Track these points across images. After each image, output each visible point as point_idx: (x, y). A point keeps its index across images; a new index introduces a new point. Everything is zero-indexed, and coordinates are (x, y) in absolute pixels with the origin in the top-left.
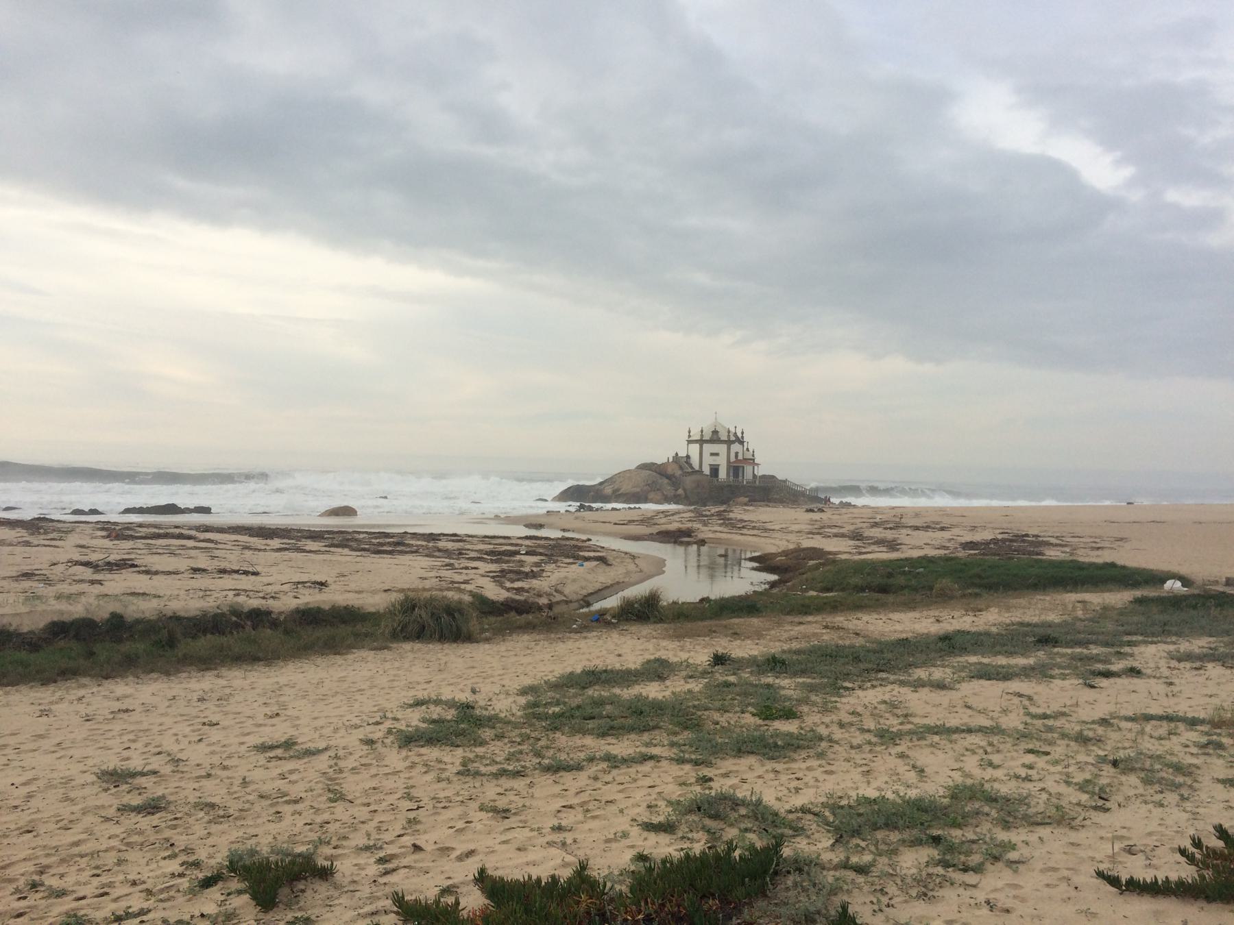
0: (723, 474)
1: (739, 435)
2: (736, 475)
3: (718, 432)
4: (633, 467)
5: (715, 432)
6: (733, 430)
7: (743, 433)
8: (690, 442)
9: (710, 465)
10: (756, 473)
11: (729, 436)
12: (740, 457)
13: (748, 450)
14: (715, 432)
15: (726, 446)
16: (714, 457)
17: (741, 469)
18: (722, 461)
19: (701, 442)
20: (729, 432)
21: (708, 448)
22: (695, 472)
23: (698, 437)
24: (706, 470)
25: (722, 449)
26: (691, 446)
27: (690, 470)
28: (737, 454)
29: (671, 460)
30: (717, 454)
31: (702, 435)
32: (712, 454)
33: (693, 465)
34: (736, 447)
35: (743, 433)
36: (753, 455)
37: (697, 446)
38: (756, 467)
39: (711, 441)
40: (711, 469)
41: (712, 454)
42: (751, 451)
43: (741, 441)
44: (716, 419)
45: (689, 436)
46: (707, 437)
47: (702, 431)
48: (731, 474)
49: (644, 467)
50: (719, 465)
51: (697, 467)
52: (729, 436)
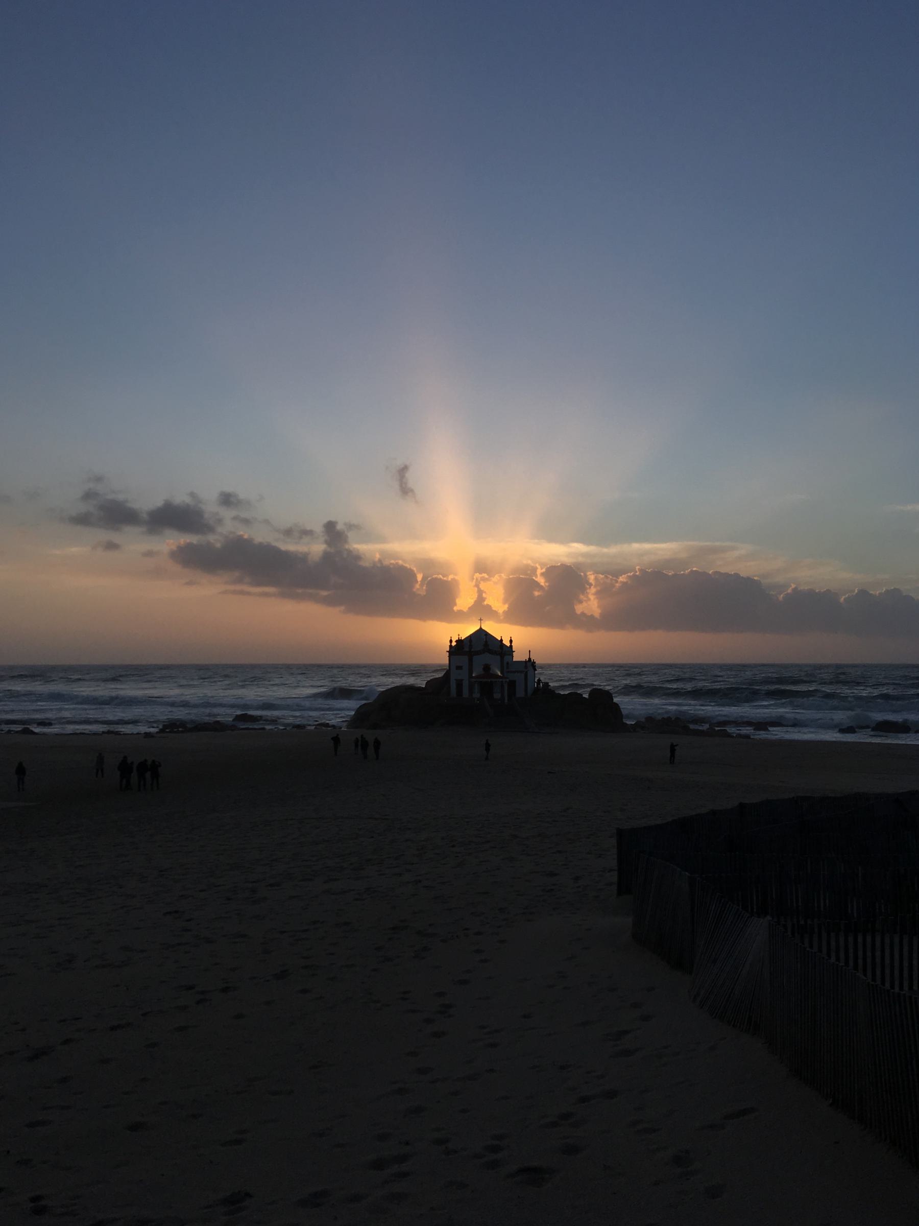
9: (456, 680)
11: (471, 647)
14: (459, 641)
25: (463, 660)
44: (481, 626)
50: (462, 680)
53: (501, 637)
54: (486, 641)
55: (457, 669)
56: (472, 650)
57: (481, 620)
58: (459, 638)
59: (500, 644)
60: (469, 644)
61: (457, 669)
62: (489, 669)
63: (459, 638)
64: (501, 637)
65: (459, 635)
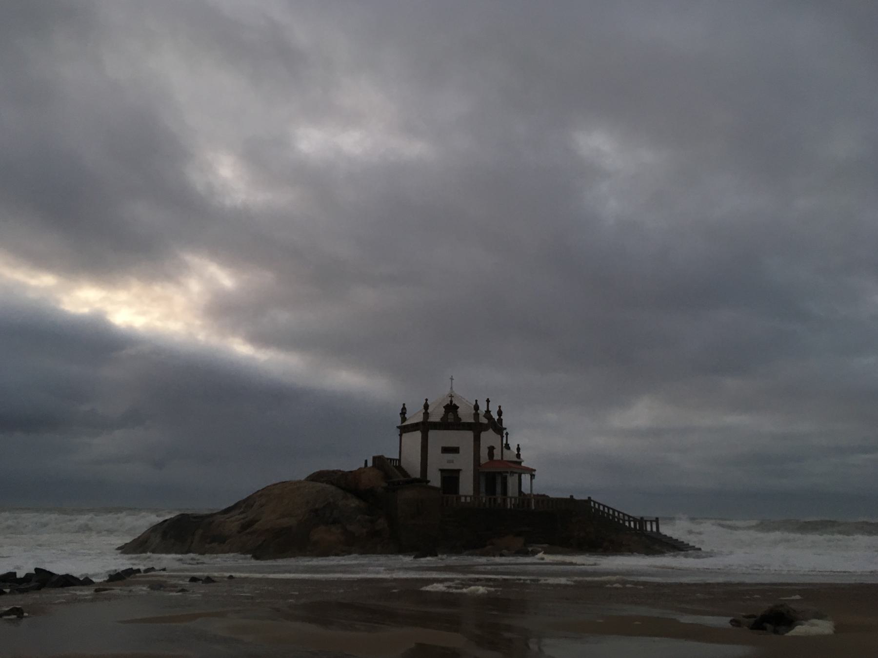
0: (466, 486)
1: (496, 417)
2: (491, 490)
3: (456, 407)
4: (303, 477)
5: (451, 408)
6: (483, 409)
7: (500, 413)
8: (404, 429)
9: (442, 471)
10: (526, 489)
11: (476, 415)
12: (497, 456)
13: (507, 447)
14: (451, 408)
15: (469, 435)
16: (450, 456)
17: (499, 481)
18: (464, 463)
19: (425, 427)
20: (476, 407)
21: (438, 439)
22: (412, 482)
23: (419, 419)
24: (435, 480)
25: (463, 439)
26: (406, 436)
27: (402, 478)
28: (491, 449)
29: (370, 464)
30: (455, 450)
31: (426, 414)
32: (446, 450)
33: (410, 472)
34: (489, 438)
35: (500, 413)
36: (518, 456)
37: (418, 435)
38: (526, 478)
39: (443, 425)
40: (444, 480)
41: (446, 450)
42: (514, 449)
43: (498, 427)
45: (404, 419)
46: (436, 415)
47: (426, 407)
48: (483, 489)
49: (319, 477)
50: (458, 471)
51: (415, 471)
52: (476, 415)
53: (500, 407)
54: (488, 412)
55: (442, 452)
56: (480, 422)
57: (452, 379)
58: (451, 401)
59: (498, 417)
60: (474, 412)
61: (442, 452)
62: (493, 454)
63: (451, 401)
64: (500, 407)
65: (451, 396)
